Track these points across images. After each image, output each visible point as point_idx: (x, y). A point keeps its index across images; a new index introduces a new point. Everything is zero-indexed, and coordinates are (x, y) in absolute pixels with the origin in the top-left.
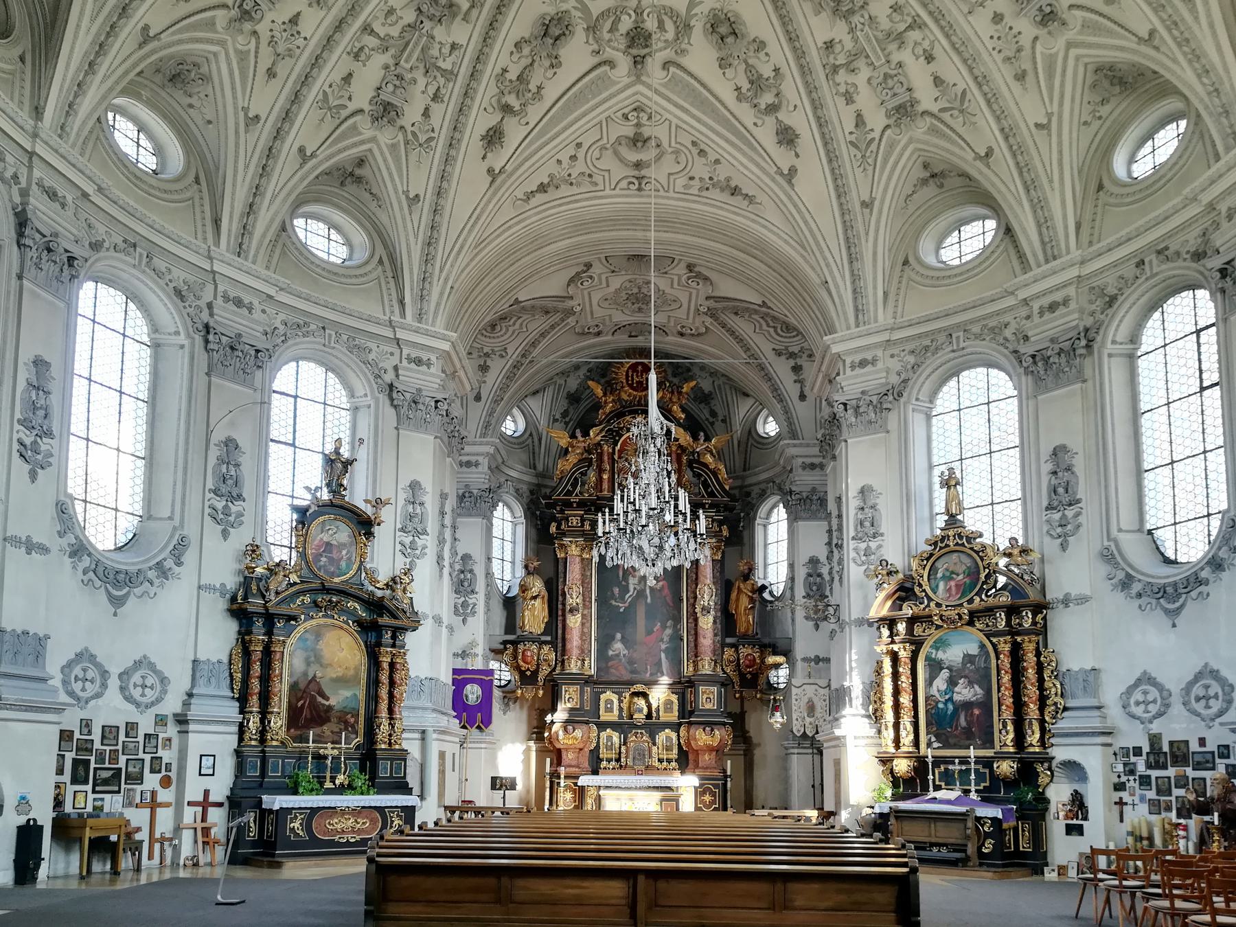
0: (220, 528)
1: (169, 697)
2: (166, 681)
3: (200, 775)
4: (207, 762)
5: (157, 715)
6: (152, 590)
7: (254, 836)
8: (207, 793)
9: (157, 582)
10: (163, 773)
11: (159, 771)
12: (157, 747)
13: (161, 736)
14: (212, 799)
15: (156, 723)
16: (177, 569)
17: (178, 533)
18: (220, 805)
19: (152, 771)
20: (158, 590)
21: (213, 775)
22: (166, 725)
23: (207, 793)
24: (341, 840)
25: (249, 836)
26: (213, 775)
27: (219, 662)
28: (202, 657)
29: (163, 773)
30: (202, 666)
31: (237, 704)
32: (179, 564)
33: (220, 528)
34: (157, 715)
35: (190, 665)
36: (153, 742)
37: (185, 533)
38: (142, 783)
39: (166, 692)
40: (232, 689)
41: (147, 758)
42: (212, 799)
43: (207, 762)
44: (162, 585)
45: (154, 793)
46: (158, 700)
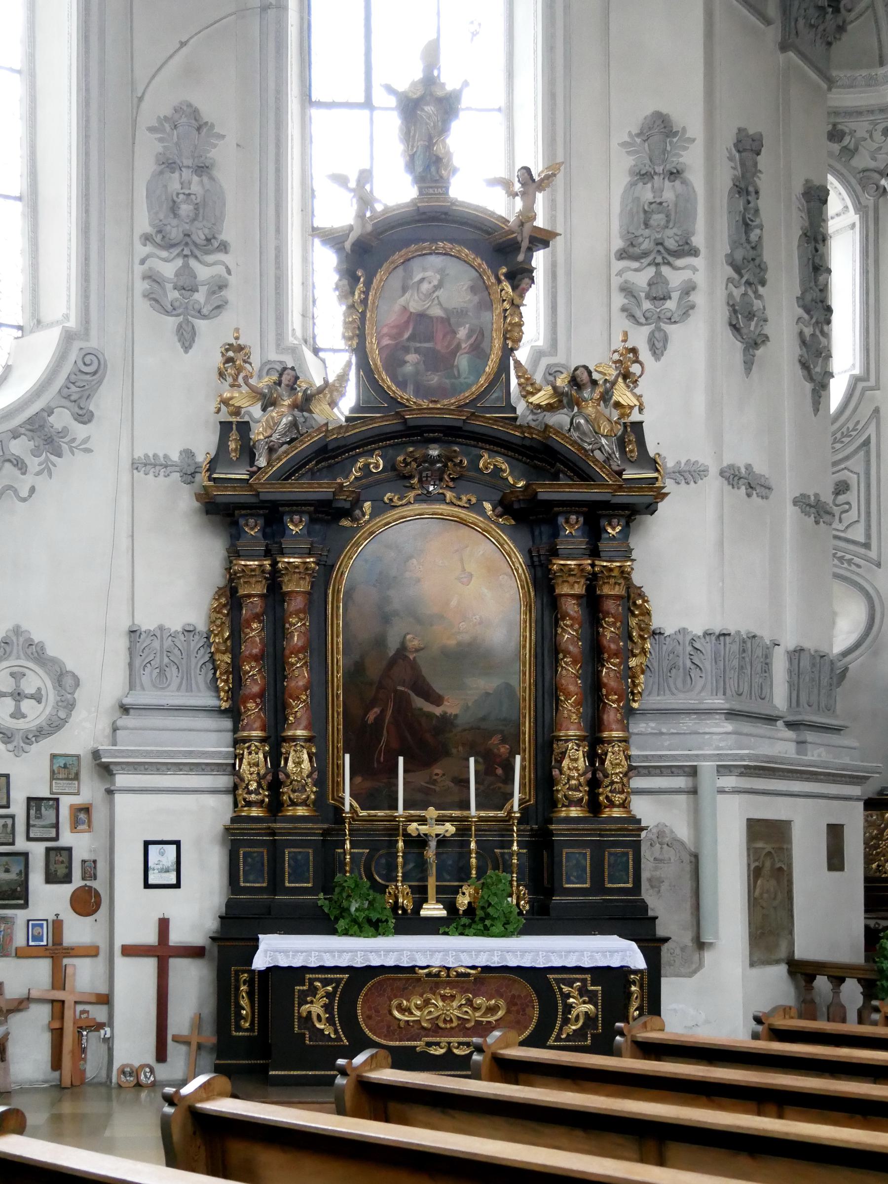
0: (171, 322)
1: (80, 715)
2: (68, 681)
3: (147, 885)
4: (163, 857)
5: (53, 757)
6: (24, 485)
7: (251, 1029)
8: (164, 925)
9: (33, 463)
10: (77, 881)
11: (67, 879)
12: (56, 826)
13: (66, 802)
14: (176, 937)
15: (53, 772)
16: (80, 431)
17: (77, 345)
18: (196, 952)
19: (51, 878)
20: (41, 483)
21: (177, 885)
22: (77, 777)
23: (164, 925)
24: (433, 1051)
25: (239, 1028)
26: (177, 885)
27: (188, 631)
28: (147, 623)
29: (77, 881)
30: (145, 641)
31: (228, 724)
32: (84, 417)
33: (171, 322)
34: (53, 757)
35: (122, 644)
36: (48, 815)
37: (93, 343)
38: (25, 905)
39: (71, 706)
40: (217, 690)
41: (37, 851)
42: (176, 937)
43: (163, 857)
44: (47, 470)
45: (57, 925)
46: (53, 726)
